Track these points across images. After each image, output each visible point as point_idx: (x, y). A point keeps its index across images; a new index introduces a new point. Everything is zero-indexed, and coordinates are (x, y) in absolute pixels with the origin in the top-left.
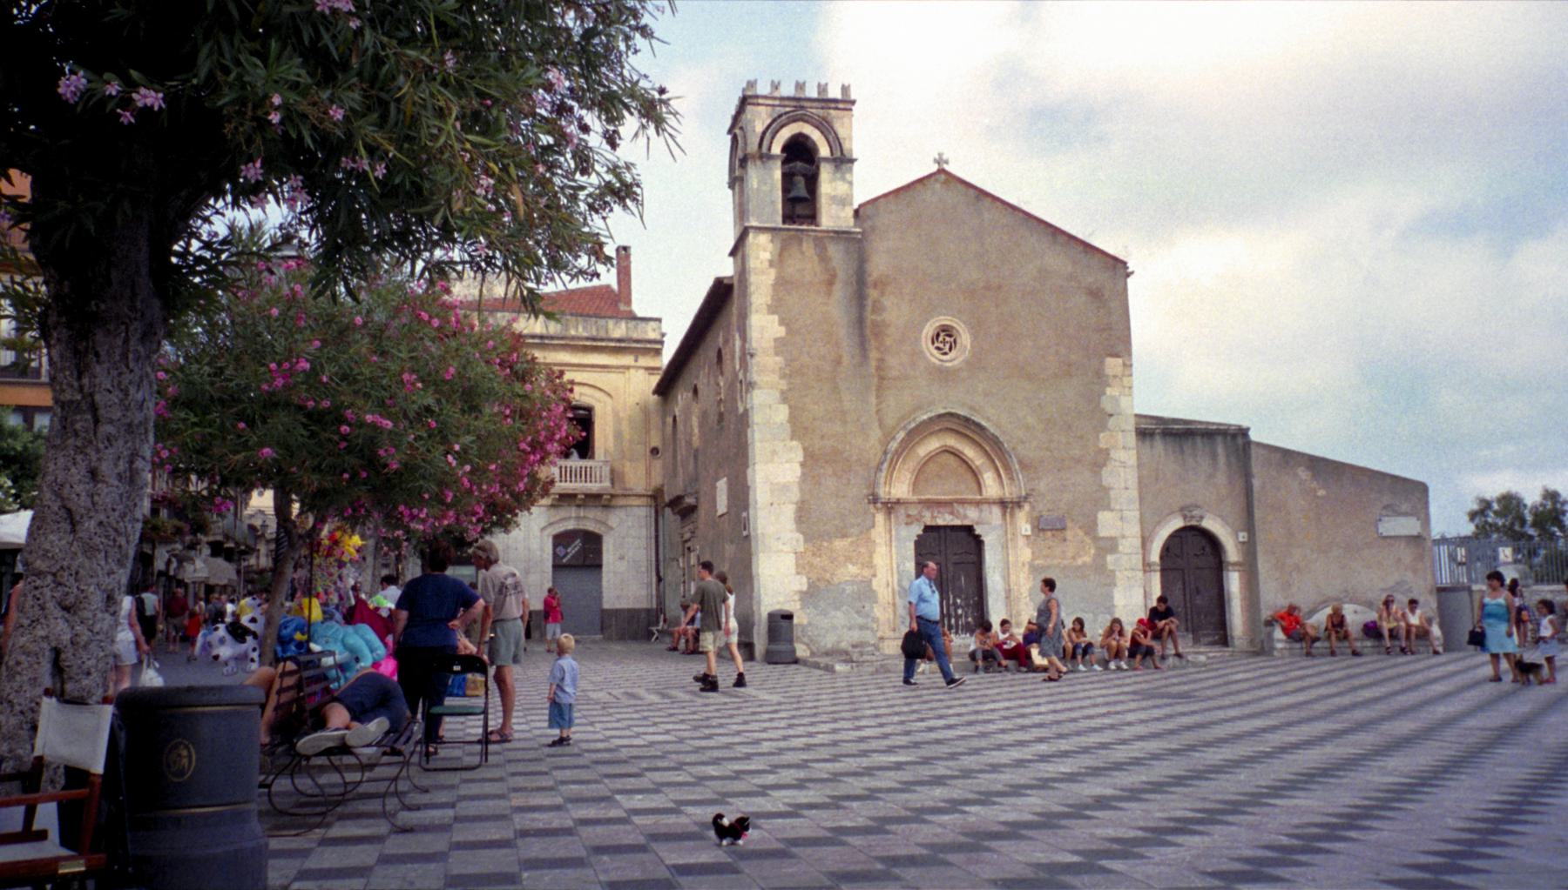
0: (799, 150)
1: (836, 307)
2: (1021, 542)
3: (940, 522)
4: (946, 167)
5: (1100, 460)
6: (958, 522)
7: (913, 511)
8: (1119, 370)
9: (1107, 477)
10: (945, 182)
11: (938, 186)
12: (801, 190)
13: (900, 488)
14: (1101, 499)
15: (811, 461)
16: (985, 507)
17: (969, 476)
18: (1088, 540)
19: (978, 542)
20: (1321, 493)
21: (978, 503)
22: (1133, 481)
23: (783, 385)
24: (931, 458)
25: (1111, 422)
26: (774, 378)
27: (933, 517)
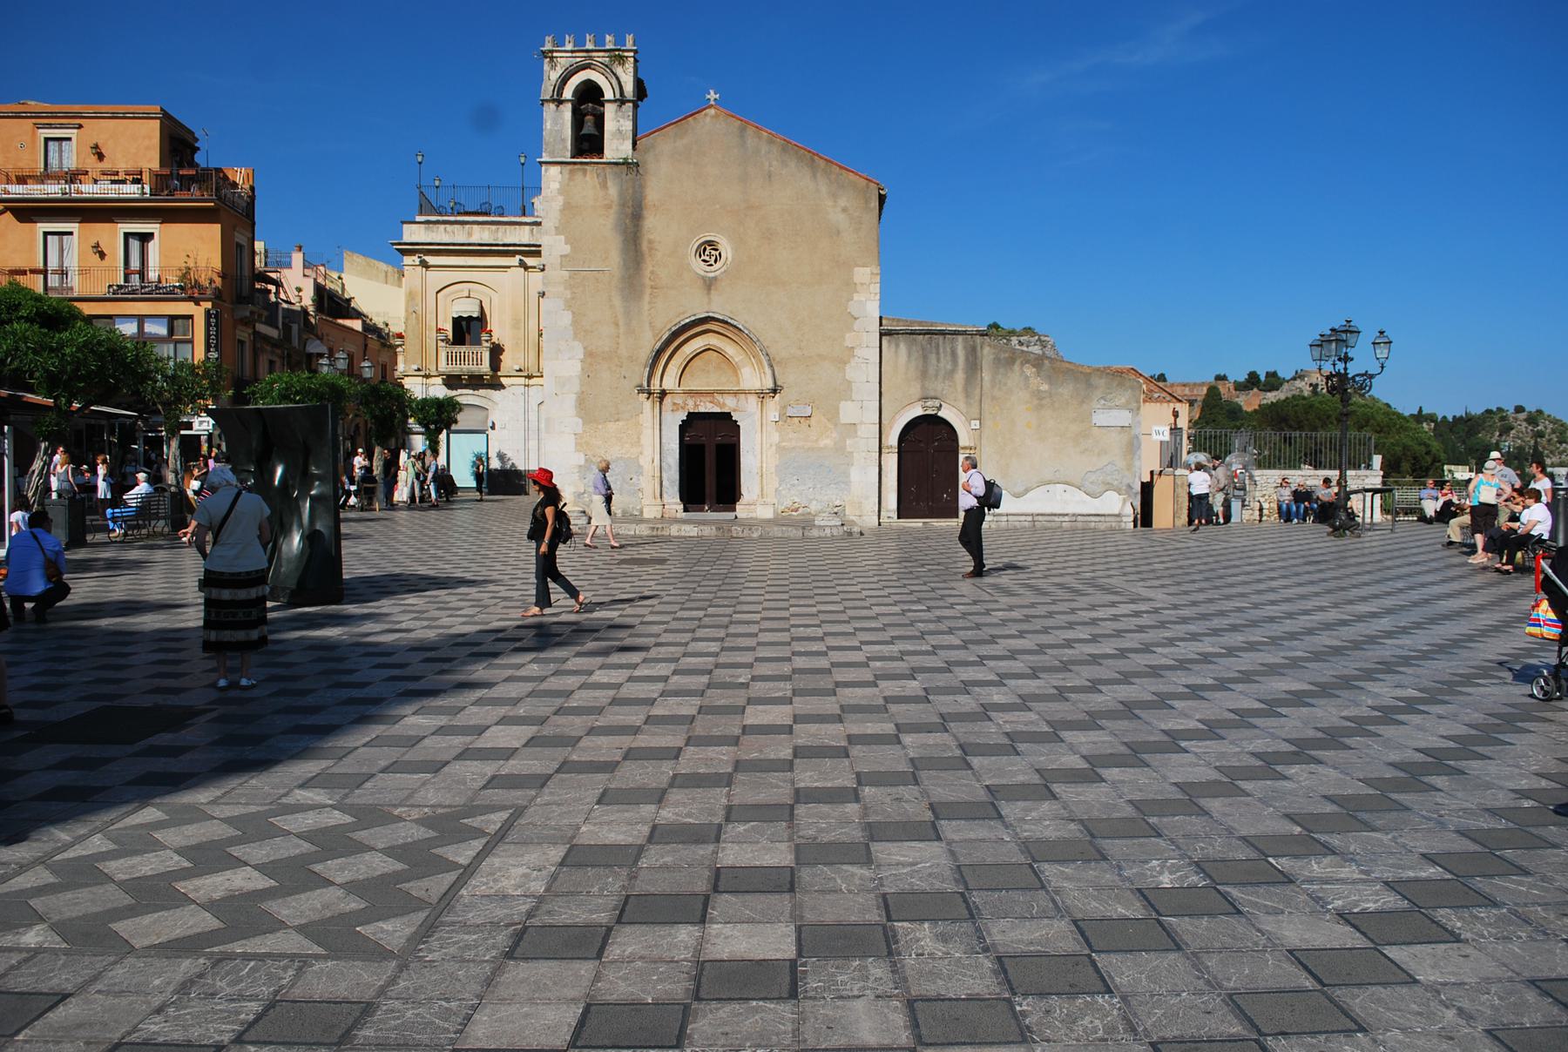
3: (702, 410)
5: (844, 358)
7: (679, 400)
9: (851, 373)
12: (589, 128)
14: (845, 391)
19: (735, 428)
20: (1045, 387)
21: (736, 393)
26: (561, 289)
27: (696, 406)
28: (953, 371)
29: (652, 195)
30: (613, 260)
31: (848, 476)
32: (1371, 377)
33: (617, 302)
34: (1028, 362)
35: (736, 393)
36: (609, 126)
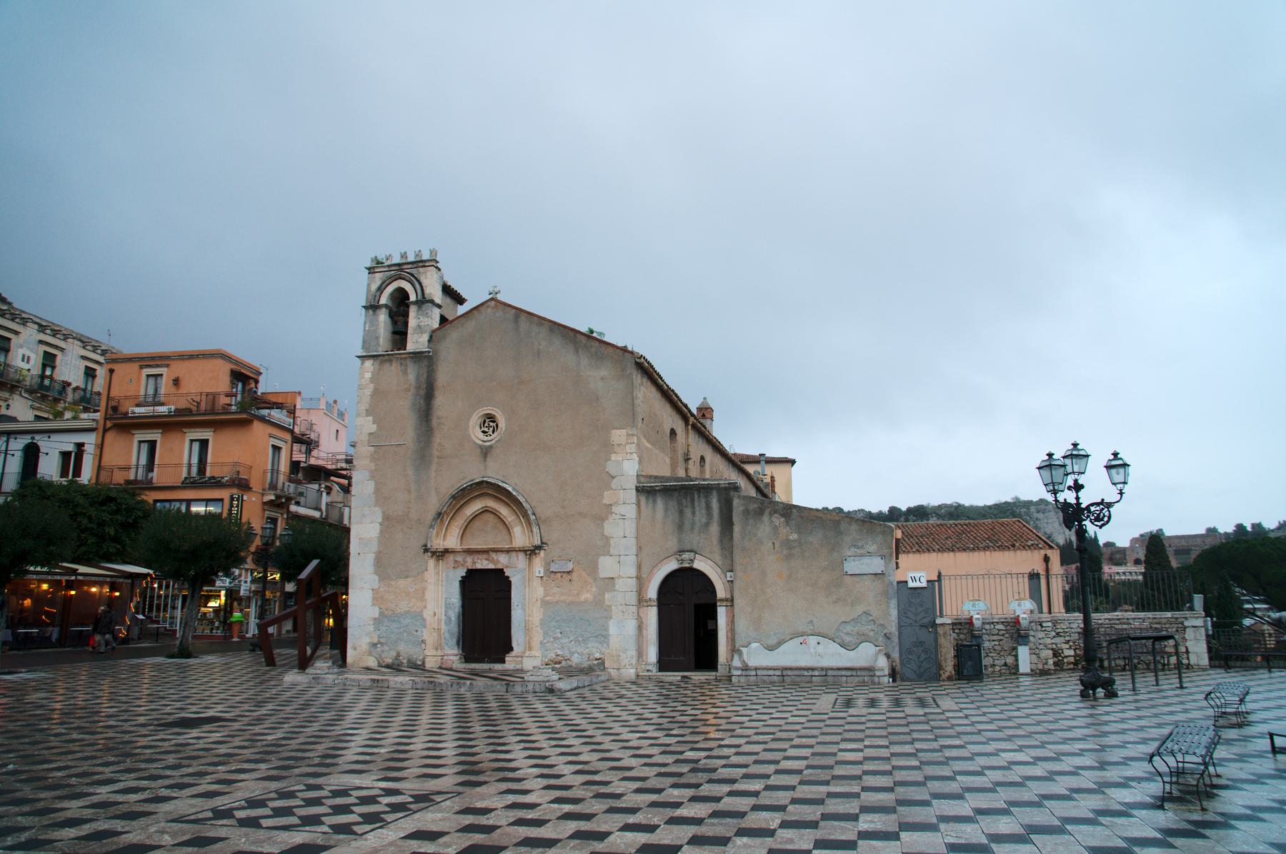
0: (401, 298)
1: (404, 408)
2: (536, 583)
3: (479, 566)
4: (499, 297)
6: (491, 566)
7: (459, 558)
8: (623, 440)
9: (609, 528)
10: (496, 307)
11: (489, 310)
12: (401, 328)
13: (452, 540)
15: (388, 522)
16: (514, 554)
17: (505, 531)
18: (590, 580)
20: (794, 536)
21: (508, 551)
22: (630, 528)
23: (372, 466)
24: (475, 517)
25: (614, 484)
26: (367, 462)
27: (474, 563)
28: (707, 525)
29: (442, 377)
30: (408, 433)
31: (607, 630)
32: (1109, 505)
33: (410, 472)
34: (776, 512)
35: (508, 551)
36: (412, 322)
